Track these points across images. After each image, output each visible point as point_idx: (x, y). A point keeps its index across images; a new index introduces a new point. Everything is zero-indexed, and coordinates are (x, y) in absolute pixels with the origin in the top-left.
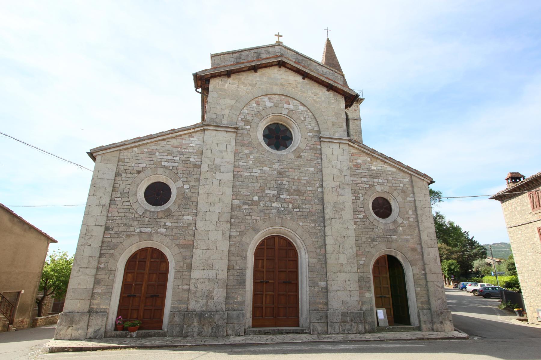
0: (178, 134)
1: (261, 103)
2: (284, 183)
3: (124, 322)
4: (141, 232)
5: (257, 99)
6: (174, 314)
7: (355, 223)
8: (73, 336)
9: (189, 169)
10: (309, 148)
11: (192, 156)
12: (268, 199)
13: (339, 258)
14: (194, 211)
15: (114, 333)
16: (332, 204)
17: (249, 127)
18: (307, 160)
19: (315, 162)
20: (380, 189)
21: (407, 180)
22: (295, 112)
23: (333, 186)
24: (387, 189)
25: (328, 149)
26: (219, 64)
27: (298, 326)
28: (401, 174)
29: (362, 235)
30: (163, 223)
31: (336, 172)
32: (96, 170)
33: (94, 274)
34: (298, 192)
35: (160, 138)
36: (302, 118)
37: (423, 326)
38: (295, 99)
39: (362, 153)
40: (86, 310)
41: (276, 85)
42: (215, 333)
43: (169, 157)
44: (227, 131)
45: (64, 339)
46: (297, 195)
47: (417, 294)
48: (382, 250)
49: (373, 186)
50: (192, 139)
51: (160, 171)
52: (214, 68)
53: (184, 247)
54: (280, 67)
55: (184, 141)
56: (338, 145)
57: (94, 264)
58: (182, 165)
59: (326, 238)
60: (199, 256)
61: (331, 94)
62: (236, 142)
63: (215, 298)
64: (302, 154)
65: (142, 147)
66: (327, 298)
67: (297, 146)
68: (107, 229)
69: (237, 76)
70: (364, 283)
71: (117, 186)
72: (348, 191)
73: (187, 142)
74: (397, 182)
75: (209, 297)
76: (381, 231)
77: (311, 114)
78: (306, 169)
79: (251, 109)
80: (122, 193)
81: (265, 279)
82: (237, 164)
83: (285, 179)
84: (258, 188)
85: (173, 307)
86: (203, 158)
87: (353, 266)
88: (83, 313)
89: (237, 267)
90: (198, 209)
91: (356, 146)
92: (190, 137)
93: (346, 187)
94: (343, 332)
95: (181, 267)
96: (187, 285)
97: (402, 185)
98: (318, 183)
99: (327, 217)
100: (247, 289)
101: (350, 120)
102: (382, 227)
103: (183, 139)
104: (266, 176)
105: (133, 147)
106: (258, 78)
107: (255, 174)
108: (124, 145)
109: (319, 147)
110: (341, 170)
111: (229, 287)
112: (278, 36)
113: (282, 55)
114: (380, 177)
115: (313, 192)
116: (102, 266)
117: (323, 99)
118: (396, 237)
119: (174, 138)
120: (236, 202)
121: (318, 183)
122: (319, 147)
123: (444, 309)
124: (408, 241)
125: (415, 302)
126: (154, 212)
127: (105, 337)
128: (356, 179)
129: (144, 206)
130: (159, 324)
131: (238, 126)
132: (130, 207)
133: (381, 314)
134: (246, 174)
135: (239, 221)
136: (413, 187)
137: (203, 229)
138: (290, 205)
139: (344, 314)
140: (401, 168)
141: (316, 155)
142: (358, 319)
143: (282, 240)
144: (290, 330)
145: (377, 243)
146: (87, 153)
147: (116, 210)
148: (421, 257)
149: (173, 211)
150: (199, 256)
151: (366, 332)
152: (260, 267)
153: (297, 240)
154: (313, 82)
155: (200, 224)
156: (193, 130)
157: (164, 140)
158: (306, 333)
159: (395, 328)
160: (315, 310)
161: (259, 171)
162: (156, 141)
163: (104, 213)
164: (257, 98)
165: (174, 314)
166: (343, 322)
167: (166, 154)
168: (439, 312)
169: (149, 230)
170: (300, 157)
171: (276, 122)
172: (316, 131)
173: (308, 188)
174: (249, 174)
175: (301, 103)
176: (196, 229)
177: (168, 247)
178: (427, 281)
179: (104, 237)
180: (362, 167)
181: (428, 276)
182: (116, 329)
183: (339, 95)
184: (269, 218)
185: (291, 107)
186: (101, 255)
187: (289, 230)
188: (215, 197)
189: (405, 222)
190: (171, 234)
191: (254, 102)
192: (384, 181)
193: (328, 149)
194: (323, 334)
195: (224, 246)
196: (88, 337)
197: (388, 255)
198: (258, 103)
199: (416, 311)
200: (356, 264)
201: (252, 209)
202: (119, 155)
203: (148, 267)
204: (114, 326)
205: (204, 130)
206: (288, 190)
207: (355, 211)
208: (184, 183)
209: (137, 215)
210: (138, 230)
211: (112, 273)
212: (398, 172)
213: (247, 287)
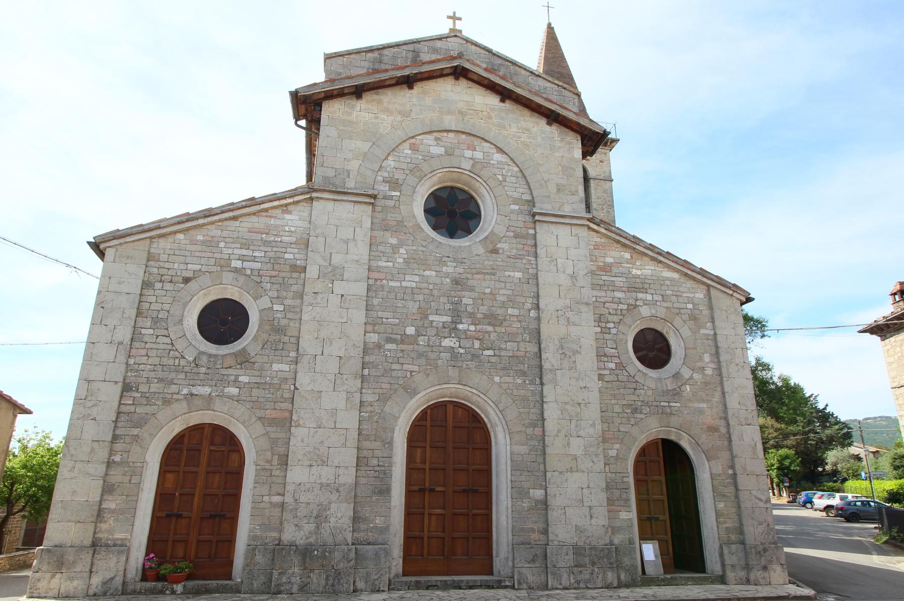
0: (262, 206)
1: (421, 148)
2: (465, 301)
3: (160, 564)
4: (192, 395)
5: (412, 141)
6: (254, 549)
7: (601, 377)
8: (62, 591)
9: (282, 275)
10: (512, 234)
11: (289, 250)
12: (434, 332)
13: (569, 444)
14: (293, 354)
15: (139, 586)
16: (556, 342)
17: (398, 194)
18: (509, 257)
19: (524, 261)
20: (648, 314)
21: (701, 296)
22: (486, 164)
23: (559, 308)
24: (662, 313)
25: (547, 236)
26: (340, 74)
27: (491, 573)
28: (690, 284)
29: (613, 402)
30: (233, 378)
31: (564, 280)
32: (106, 276)
33: (103, 474)
34: (492, 319)
35: (226, 215)
36: (500, 178)
37: (730, 575)
38: (486, 141)
39: (615, 245)
40: (88, 541)
41: (450, 112)
42: (333, 585)
43: (244, 252)
44: (355, 202)
45: (45, 597)
46: (489, 324)
47: (718, 514)
48: (651, 429)
49: (636, 306)
50: (287, 217)
51: (228, 277)
52: (330, 81)
53: (273, 422)
54: (457, 79)
55: (272, 221)
56: (568, 228)
57: (103, 454)
58: (269, 266)
59: (545, 406)
60: (302, 441)
61: (554, 131)
62: (372, 223)
63: (333, 520)
64: (499, 246)
65: (191, 232)
66: (547, 520)
67: (490, 230)
68: (127, 388)
69: (375, 97)
70: (617, 493)
71: (145, 306)
72: (588, 316)
73: (278, 222)
74: (681, 300)
75: (320, 518)
76: (650, 393)
77: (516, 169)
78: (507, 273)
79: (402, 159)
80: (156, 321)
81: (427, 485)
82: (373, 264)
83: (467, 293)
84: (415, 311)
85: (253, 537)
86: (310, 254)
87: (595, 460)
88: (81, 548)
89: (375, 462)
90: (301, 350)
91: (603, 231)
92: (284, 212)
93: (584, 308)
94: (576, 585)
95: (268, 461)
96: (279, 494)
97: (690, 306)
98: (530, 300)
99: (546, 365)
100: (393, 504)
101: (592, 181)
102: (653, 386)
103: (270, 217)
104: (431, 287)
105: (175, 232)
106: (414, 100)
107: (408, 284)
108: (159, 228)
109: (532, 232)
110: (573, 277)
111: (358, 500)
112: (454, 18)
113: (460, 56)
114: (649, 291)
115: (520, 318)
116: (117, 458)
117: (539, 139)
118: (678, 404)
119: (254, 214)
120: (373, 338)
121: (530, 300)
122: (532, 232)
123: (771, 543)
124: (701, 412)
125: (715, 528)
126: (216, 356)
127: (122, 594)
128: (603, 294)
129: (197, 345)
130: (225, 569)
131: (376, 192)
132: (170, 347)
133: (650, 551)
134: (392, 284)
135: (378, 374)
136: (711, 308)
137: (309, 388)
138: (477, 344)
139: (578, 550)
140: (689, 272)
141: (526, 248)
142: (605, 560)
143: (460, 411)
144: (476, 581)
145: (643, 416)
146: (89, 243)
147: (143, 352)
148: (726, 443)
149: (252, 354)
150: (302, 441)
151: (620, 585)
152: (418, 460)
153: (490, 410)
154: (521, 108)
155: (304, 380)
156: (291, 200)
157: (235, 218)
158: (506, 587)
159: (676, 578)
160: (523, 544)
161: (417, 279)
162: (220, 221)
163: (122, 358)
164: (412, 137)
165: (254, 549)
166: (576, 566)
167: (239, 246)
168: (760, 548)
169: (206, 390)
170: (495, 251)
171: (449, 184)
172: (527, 201)
173: (510, 311)
174: (397, 284)
175: (497, 147)
176: (296, 388)
177: (243, 423)
178: (737, 489)
179: (120, 404)
180: (615, 270)
181: (741, 479)
182: (144, 578)
183: (571, 133)
184: (436, 367)
185: (478, 155)
186: (115, 438)
187: (475, 391)
188: (331, 328)
189: (696, 376)
190: (248, 399)
191: (407, 145)
192: (656, 298)
193: (547, 236)
194: (538, 588)
195: (350, 420)
196: (91, 592)
197: (662, 439)
198: (414, 148)
199: (717, 545)
200: (601, 457)
201: (402, 351)
202: (150, 247)
203: (204, 459)
204: (140, 573)
205: (311, 199)
206: (472, 315)
207: (601, 355)
208: (274, 301)
209: (183, 362)
210: (185, 391)
211: (137, 471)
212: (683, 279)
213: (393, 500)
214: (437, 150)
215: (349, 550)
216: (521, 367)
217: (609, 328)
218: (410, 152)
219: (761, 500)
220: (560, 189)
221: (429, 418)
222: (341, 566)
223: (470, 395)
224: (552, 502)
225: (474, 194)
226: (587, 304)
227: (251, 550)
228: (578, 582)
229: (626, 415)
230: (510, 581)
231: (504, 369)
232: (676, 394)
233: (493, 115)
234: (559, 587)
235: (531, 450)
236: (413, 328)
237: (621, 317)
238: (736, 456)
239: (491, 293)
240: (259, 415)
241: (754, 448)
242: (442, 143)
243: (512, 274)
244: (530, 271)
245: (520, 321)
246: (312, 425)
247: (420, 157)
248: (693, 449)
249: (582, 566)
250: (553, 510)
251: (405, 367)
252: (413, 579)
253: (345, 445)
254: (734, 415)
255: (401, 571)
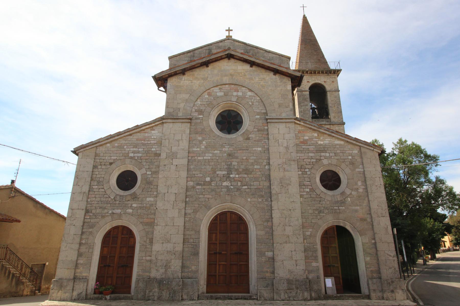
0: (142, 129)
1: (213, 94)
2: (233, 163)
3: (101, 286)
4: (113, 213)
5: (209, 91)
6: (139, 281)
7: (301, 196)
8: (62, 297)
9: (151, 158)
10: (256, 130)
11: (154, 147)
12: (219, 179)
13: (285, 230)
14: (155, 193)
15: (92, 296)
16: (278, 180)
17: (202, 116)
18: (255, 141)
19: (263, 142)
20: (327, 163)
21: (356, 152)
22: (244, 97)
23: (280, 163)
24: (334, 162)
25: (274, 129)
26: (175, 65)
28: (350, 146)
29: (308, 208)
30: (130, 205)
31: (282, 149)
32: (79, 164)
33: (77, 248)
34: (247, 171)
35: (127, 134)
36: (250, 103)
37: (373, 295)
38: (244, 87)
39: (309, 130)
40: (72, 277)
41: (226, 76)
42: (172, 297)
43: (135, 149)
44: (182, 122)
45: (55, 300)
46: (245, 174)
47: (366, 263)
48: (329, 221)
49: (320, 160)
50: (153, 132)
51: (128, 161)
52: (170, 69)
53: (147, 224)
54: (229, 59)
55: (146, 135)
56: (284, 124)
57: (78, 240)
58: (145, 155)
59: (273, 211)
60: (159, 232)
61: (277, 77)
62: (190, 131)
63: (172, 267)
64: (250, 136)
65: (113, 143)
66: (274, 267)
67: (245, 129)
68: (87, 211)
69: (191, 73)
70: (310, 253)
71: (94, 176)
72: (294, 166)
73: (149, 135)
74: (345, 155)
75: (167, 266)
76: (328, 203)
77: (258, 98)
78: (254, 149)
79: (204, 100)
80: (99, 182)
82: (191, 150)
83: (234, 160)
84: (210, 170)
85: (138, 275)
86: (162, 148)
87: (299, 237)
88: (69, 280)
89: (192, 241)
90: (158, 191)
91: (302, 124)
92: (151, 130)
93: (292, 163)
94: (288, 299)
95: (145, 241)
96: (149, 256)
97: (350, 157)
98: (265, 161)
99: (273, 192)
100: (200, 260)
102: (330, 199)
103: (146, 133)
104: (217, 158)
105: (106, 143)
106: (209, 72)
107: (207, 158)
108: (99, 142)
109: (266, 128)
110: (287, 148)
111: (184, 258)
112: (229, 30)
113: (229, 49)
114: (327, 151)
115: (260, 170)
116: (84, 242)
117: (270, 83)
118: (344, 208)
119: (139, 132)
120: (191, 184)
121: (265, 161)
122: (266, 128)
123: (396, 278)
124: (356, 211)
125: (365, 270)
126: (123, 196)
127: (86, 299)
128: (303, 155)
129: (115, 192)
130: (128, 289)
131: (191, 117)
132: (104, 193)
133: (329, 282)
134: (199, 158)
135: (193, 200)
136: (362, 158)
137: (162, 208)
138: (239, 184)
139: (289, 282)
140: (349, 140)
141: (264, 136)
142: (304, 286)
144: (239, 296)
145: (324, 214)
146: (72, 151)
147: (94, 196)
148: (371, 227)
149: (138, 194)
150: (159, 232)
151: (311, 299)
153: (246, 214)
154: (260, 68)
155: (160, 204)
156: (154, 124)
157: (130, 135)
158: (254, 299)
159: (343, 296)
160: (262, 278)
161: (211, 155)
162: (124, 136)
163: (85, 199)
164: (209, 89)
165: (139, 281)
166: (288, 289)
167: (132, 147)
168: (390, 281)
169: (119, 211)
170: (248, 139)
171: (227, 109)
172: (264, 113)
173: (255, 167)
174: (202, 158)
175: (249, 89)
176: (157, 209)
177: (134, 225)
178: (377, 251)
179: (84, 218)
180: (309, 142)
181: (378, 245)
182: (95, 293)
183: (286, 78)
184: (220, 196)
185: (240, 94)
186: (83, 233)
187: (238, 206)
188: (171, 181)
189: (354, 193)
190: (137, 214)
191: (206, 93)
192: (331, 155)
193: (274, 129)
194: (270, 300)
195: (180, 222)
196: (73, 298)
197: (336, 226)
198: (209, 94)
199: (366, 280)
200: (302, 236)
201: (204, 189)
202: (96, 150)
203: (119, 242)
204: (93, 291)
205: (163, 123)
206: (237, 170)
207: (301, 185)
208: (147, 170)
209: (109, 199)
210: (110, 212)
211: (91, 247)
212: (346, 144)
213: (200, 258)
214: (220, 94)
215: (180, 281)
216: (261, 193)
217: (306, 172)
218: (207, 96)
219: (391, 256)
220: (280, 105)
221: (218, 220)
222: (176, 288)
223: (237, 208)
224: (276, 258)
225: (239, 112)
226: (294, 160)
227: (138, 281)
228: (290, 297)
229: (315, 214)
230: (256, 296)
231: (253, 195)
232: (343, 203)
233: (247, 74)
234: (280, 299)
235: (266, 233)
236: (209, 178)
237: (312, 166)
238: (376, 233)
239: (246, 159)
240: (141, 221)
241: (387, 229)
242: (222, 90)
243: (256, 149)
244: (266, 147)
245: (260, 171)
246: (163, 225)
247: (212, 98)
248: (353, 230)
249: (291, 289)
250: (277, 262)
251: (206, 196)
252: (209, 295)
253: (178, 233)
254: (374, 212)
255: (205, 291)
